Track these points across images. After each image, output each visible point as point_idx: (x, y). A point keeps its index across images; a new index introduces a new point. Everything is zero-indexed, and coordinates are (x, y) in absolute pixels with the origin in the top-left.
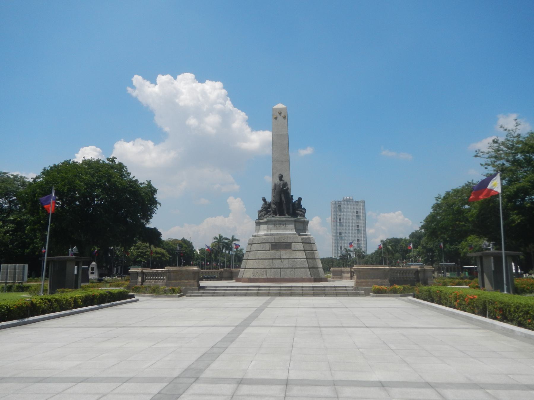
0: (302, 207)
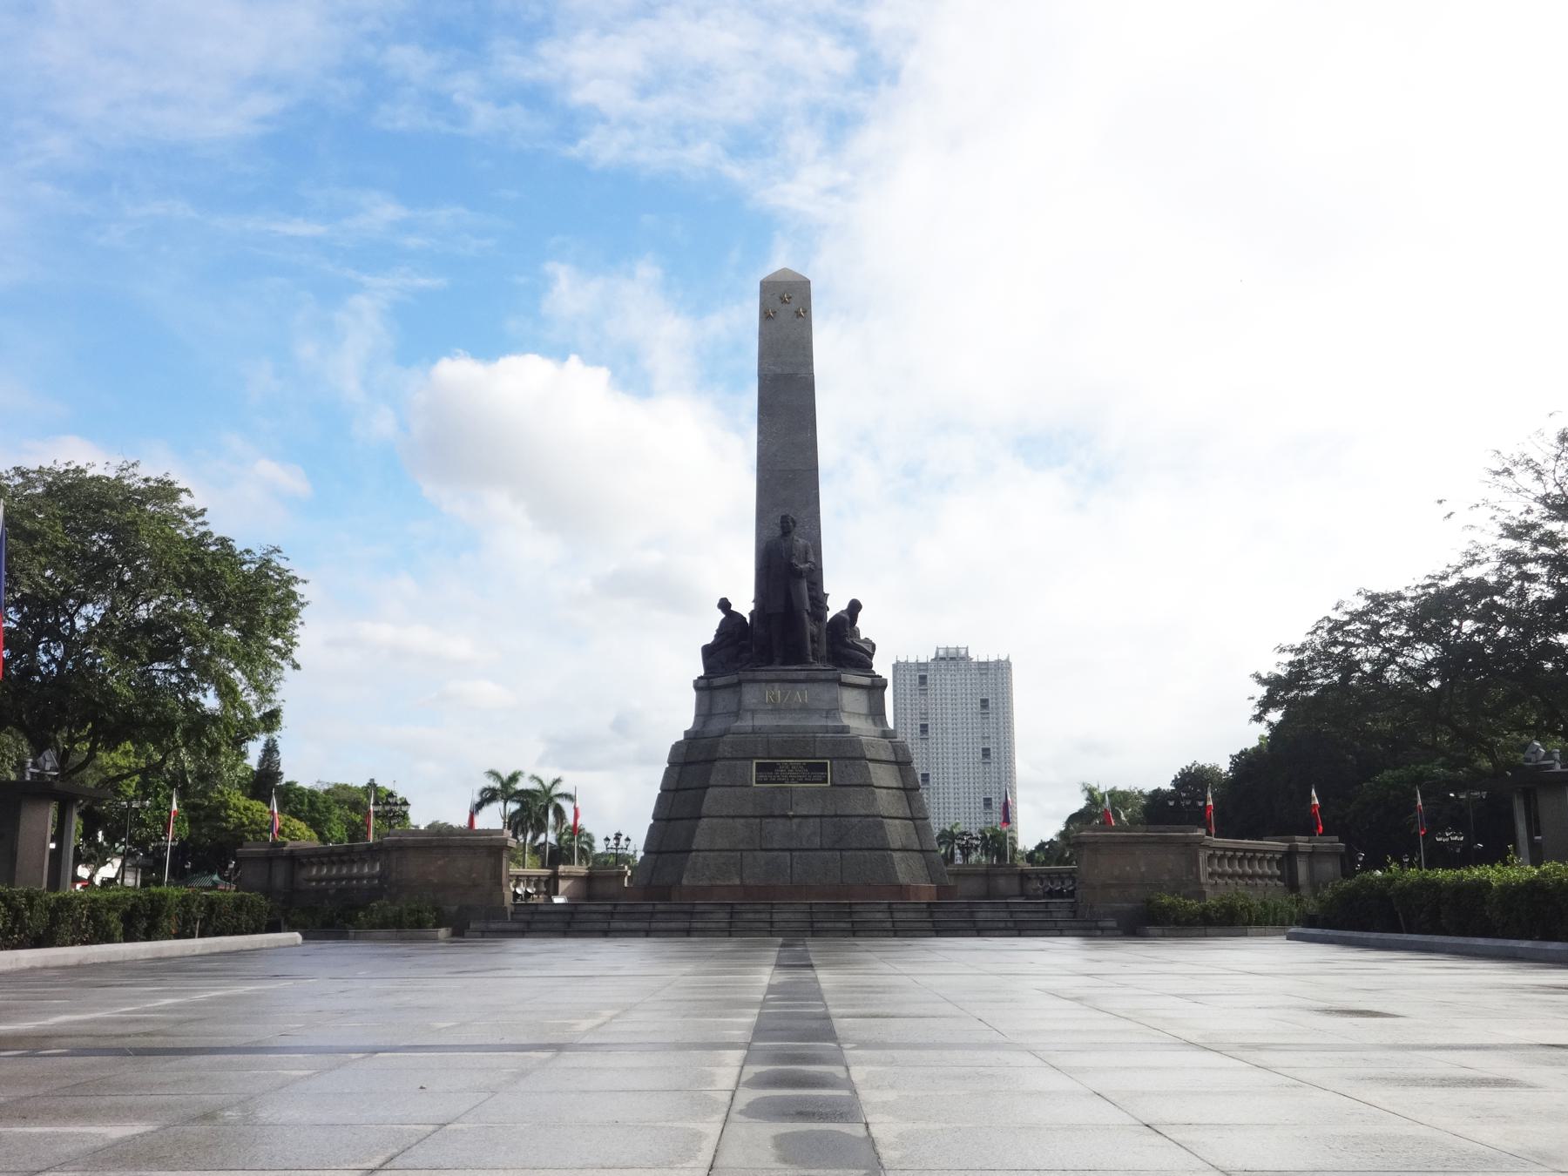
0: (862, 637)
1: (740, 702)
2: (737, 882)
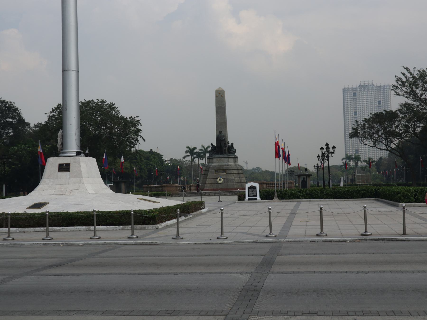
1: (213, 161)
2: (212, 188)
